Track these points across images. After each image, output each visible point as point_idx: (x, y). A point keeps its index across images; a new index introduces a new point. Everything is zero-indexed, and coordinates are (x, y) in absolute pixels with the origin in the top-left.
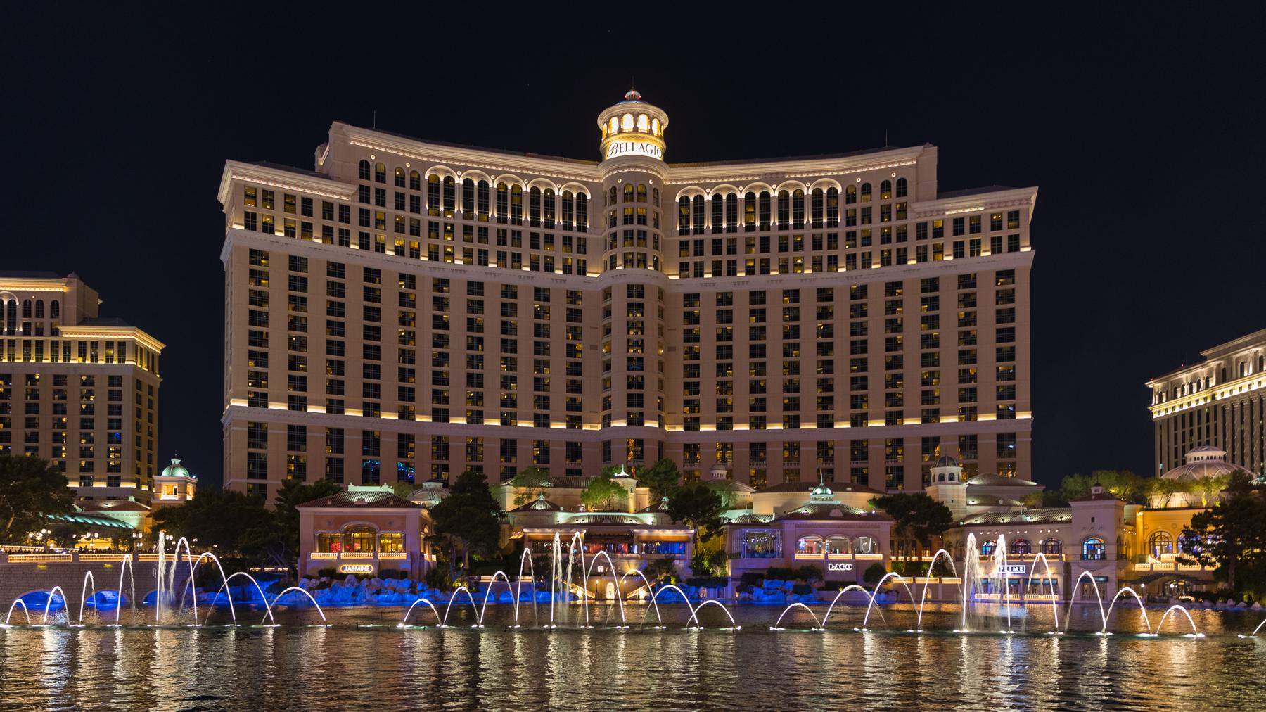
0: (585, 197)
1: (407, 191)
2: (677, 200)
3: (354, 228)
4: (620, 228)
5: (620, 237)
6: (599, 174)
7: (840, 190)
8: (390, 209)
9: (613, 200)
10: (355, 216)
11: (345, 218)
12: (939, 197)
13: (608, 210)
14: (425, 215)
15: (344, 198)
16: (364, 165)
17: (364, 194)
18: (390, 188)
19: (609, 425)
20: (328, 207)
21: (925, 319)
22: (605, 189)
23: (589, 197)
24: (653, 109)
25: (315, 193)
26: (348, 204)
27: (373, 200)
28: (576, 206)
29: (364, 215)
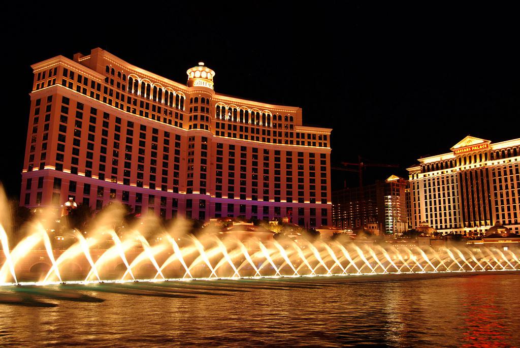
2: (216, 106)
4: (199, 114)
5: (199, 118)
7: (271, 115)
8: (115, 89)
9: (191, 102)
10: (102, 89)
11: (99, 89)
12: (304, 125)
13: (193, 105)
14: (126, 95)
16: (108, 68)
17: (107, 80)
19: (191, 192)
20: (93, 82)
22: (191, 97)
23: (185, 98)
24: (207, 69)
26: (101, 83)
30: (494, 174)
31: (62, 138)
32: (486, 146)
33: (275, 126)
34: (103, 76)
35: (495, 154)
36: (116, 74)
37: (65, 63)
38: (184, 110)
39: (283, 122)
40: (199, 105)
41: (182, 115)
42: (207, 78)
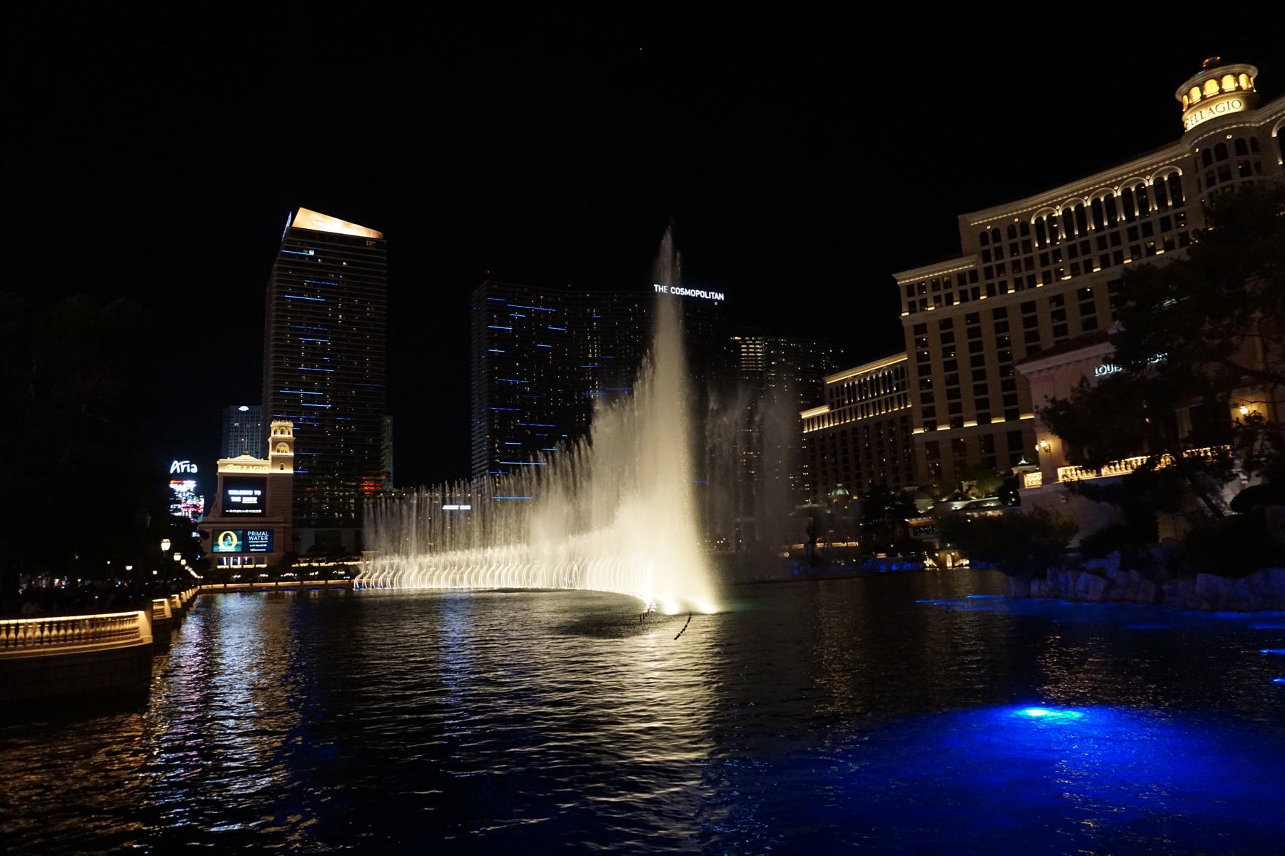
0: (1178, 174)
1: (1019, 239)
2: (1274, 135)
3: (982, 283)
6: (1182, 150)
8: (1008, 259)
10: (981, 275)
14: (1035, 254)
15: (971, 266)
16: (984, 236)
17: (986, 256)
18: (1005, 242)
21: (1054, 314)
23: (1181, 174)
25: (950, 271)
27: (993, 258)
29: (988, 273)
34: (973, 256)
36: (1004, 234)
37: (905, 279)
42: (1203, 98)
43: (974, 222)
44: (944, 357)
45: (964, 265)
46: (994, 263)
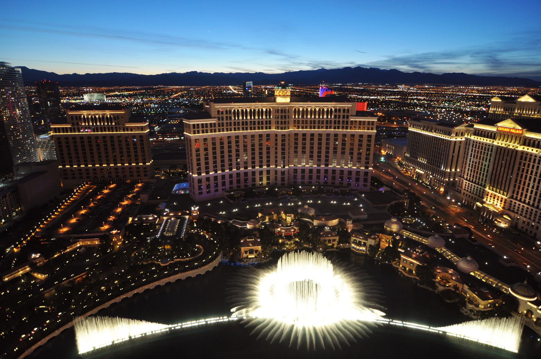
1: (228, 115)
6: (274, 105)
7: (333, 110)
8: (225, 121)
10: (217, 125)
11: (215, 126)
14: (232, 122)
23: (272, 110)
28: (268, 113)
29: (219, 124)
30: (522, 157)
31: (198, 160)
32: (521, 132)
33: (335, 116)
35: (527, 141)
36: (224, 113)
38: (271, 117)
39: (342, 114)
40: (280, 114)
41: (270, 122)
43: (216, 106)
44: (208, 153)
45: (213, 121)
46: (221, 122)
